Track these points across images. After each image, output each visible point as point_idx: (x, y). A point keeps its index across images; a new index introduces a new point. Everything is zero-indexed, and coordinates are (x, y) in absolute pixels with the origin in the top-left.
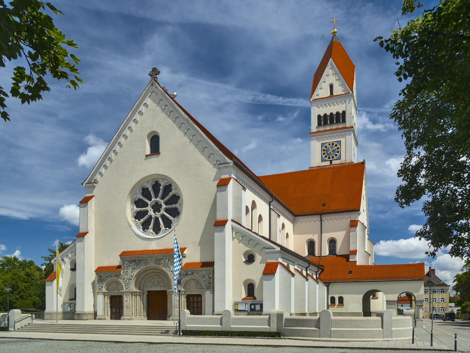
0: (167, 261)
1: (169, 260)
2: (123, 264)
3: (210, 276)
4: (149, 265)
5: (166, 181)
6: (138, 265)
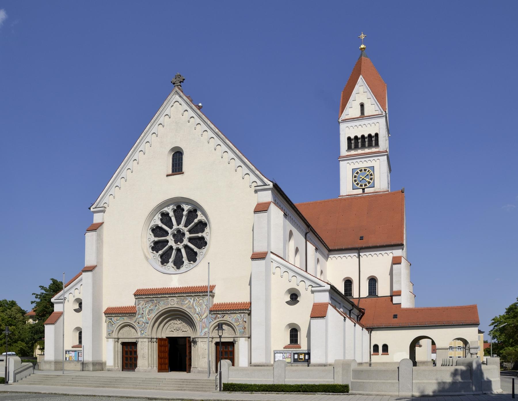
0: (192, 301)
1: (194, 300)
3: (245, 320)
4: (170, 306)
6: (156, 306)
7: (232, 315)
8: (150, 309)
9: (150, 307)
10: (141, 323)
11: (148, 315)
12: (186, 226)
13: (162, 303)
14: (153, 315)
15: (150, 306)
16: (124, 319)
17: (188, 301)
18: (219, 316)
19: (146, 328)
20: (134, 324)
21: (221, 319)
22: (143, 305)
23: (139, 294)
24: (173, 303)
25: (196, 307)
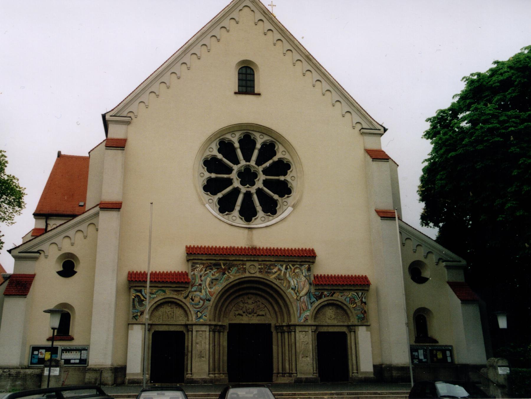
0: (283, 269)
1: (286, 269)
2: (193, 270)
4: (247, 275)
5: (266, 138)
6: (224, 274)
7: (346, 293)
8: (214, 277)
9: (213, 275)
10: (197, 299)
11: (210, 288)
12: (259, 162)
13: (234, 269)
14: (218, 288)
15: (213, 274)
16: (164, 292)
17: (277, 268)
18: (326, 293)
19: (207, 307)
20: (184, 300)
21: (330, 298)
22: (202, 270)
23: (194, 254)
24: (253, 270)
25: (290, 279)
